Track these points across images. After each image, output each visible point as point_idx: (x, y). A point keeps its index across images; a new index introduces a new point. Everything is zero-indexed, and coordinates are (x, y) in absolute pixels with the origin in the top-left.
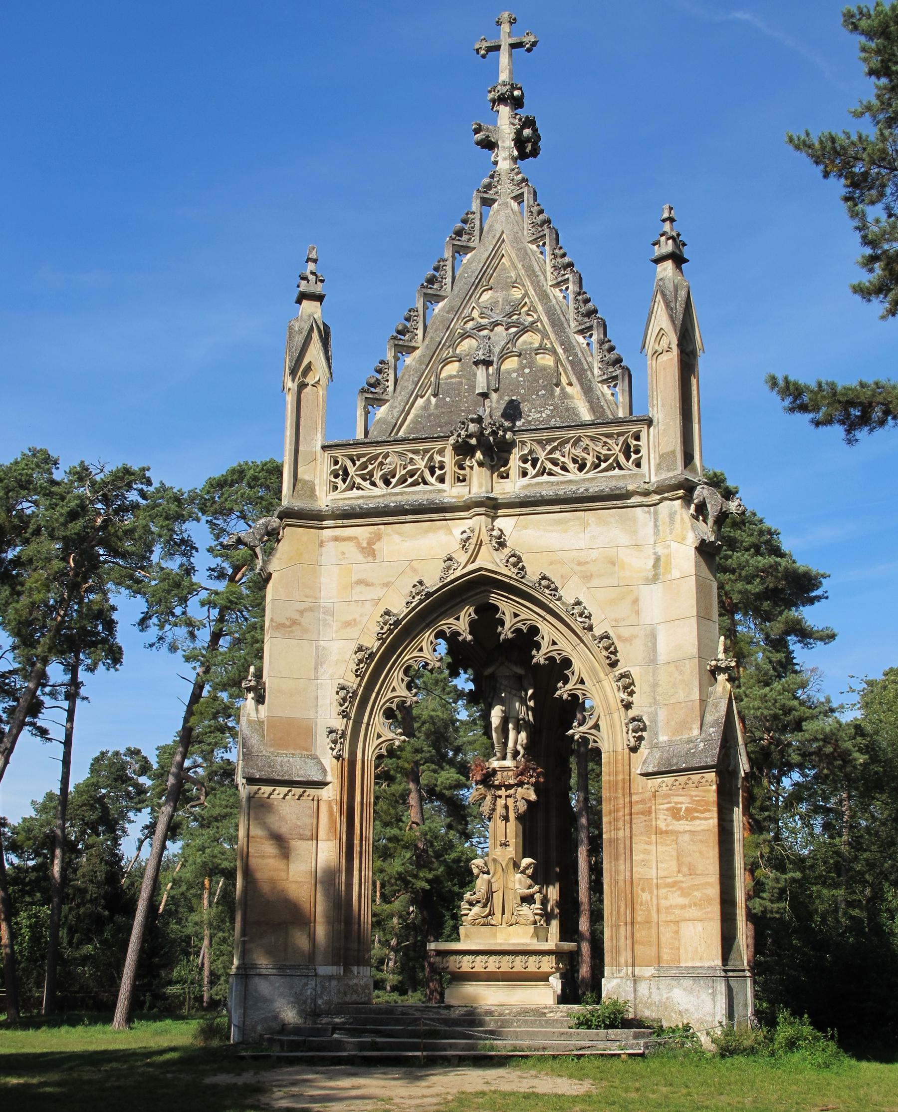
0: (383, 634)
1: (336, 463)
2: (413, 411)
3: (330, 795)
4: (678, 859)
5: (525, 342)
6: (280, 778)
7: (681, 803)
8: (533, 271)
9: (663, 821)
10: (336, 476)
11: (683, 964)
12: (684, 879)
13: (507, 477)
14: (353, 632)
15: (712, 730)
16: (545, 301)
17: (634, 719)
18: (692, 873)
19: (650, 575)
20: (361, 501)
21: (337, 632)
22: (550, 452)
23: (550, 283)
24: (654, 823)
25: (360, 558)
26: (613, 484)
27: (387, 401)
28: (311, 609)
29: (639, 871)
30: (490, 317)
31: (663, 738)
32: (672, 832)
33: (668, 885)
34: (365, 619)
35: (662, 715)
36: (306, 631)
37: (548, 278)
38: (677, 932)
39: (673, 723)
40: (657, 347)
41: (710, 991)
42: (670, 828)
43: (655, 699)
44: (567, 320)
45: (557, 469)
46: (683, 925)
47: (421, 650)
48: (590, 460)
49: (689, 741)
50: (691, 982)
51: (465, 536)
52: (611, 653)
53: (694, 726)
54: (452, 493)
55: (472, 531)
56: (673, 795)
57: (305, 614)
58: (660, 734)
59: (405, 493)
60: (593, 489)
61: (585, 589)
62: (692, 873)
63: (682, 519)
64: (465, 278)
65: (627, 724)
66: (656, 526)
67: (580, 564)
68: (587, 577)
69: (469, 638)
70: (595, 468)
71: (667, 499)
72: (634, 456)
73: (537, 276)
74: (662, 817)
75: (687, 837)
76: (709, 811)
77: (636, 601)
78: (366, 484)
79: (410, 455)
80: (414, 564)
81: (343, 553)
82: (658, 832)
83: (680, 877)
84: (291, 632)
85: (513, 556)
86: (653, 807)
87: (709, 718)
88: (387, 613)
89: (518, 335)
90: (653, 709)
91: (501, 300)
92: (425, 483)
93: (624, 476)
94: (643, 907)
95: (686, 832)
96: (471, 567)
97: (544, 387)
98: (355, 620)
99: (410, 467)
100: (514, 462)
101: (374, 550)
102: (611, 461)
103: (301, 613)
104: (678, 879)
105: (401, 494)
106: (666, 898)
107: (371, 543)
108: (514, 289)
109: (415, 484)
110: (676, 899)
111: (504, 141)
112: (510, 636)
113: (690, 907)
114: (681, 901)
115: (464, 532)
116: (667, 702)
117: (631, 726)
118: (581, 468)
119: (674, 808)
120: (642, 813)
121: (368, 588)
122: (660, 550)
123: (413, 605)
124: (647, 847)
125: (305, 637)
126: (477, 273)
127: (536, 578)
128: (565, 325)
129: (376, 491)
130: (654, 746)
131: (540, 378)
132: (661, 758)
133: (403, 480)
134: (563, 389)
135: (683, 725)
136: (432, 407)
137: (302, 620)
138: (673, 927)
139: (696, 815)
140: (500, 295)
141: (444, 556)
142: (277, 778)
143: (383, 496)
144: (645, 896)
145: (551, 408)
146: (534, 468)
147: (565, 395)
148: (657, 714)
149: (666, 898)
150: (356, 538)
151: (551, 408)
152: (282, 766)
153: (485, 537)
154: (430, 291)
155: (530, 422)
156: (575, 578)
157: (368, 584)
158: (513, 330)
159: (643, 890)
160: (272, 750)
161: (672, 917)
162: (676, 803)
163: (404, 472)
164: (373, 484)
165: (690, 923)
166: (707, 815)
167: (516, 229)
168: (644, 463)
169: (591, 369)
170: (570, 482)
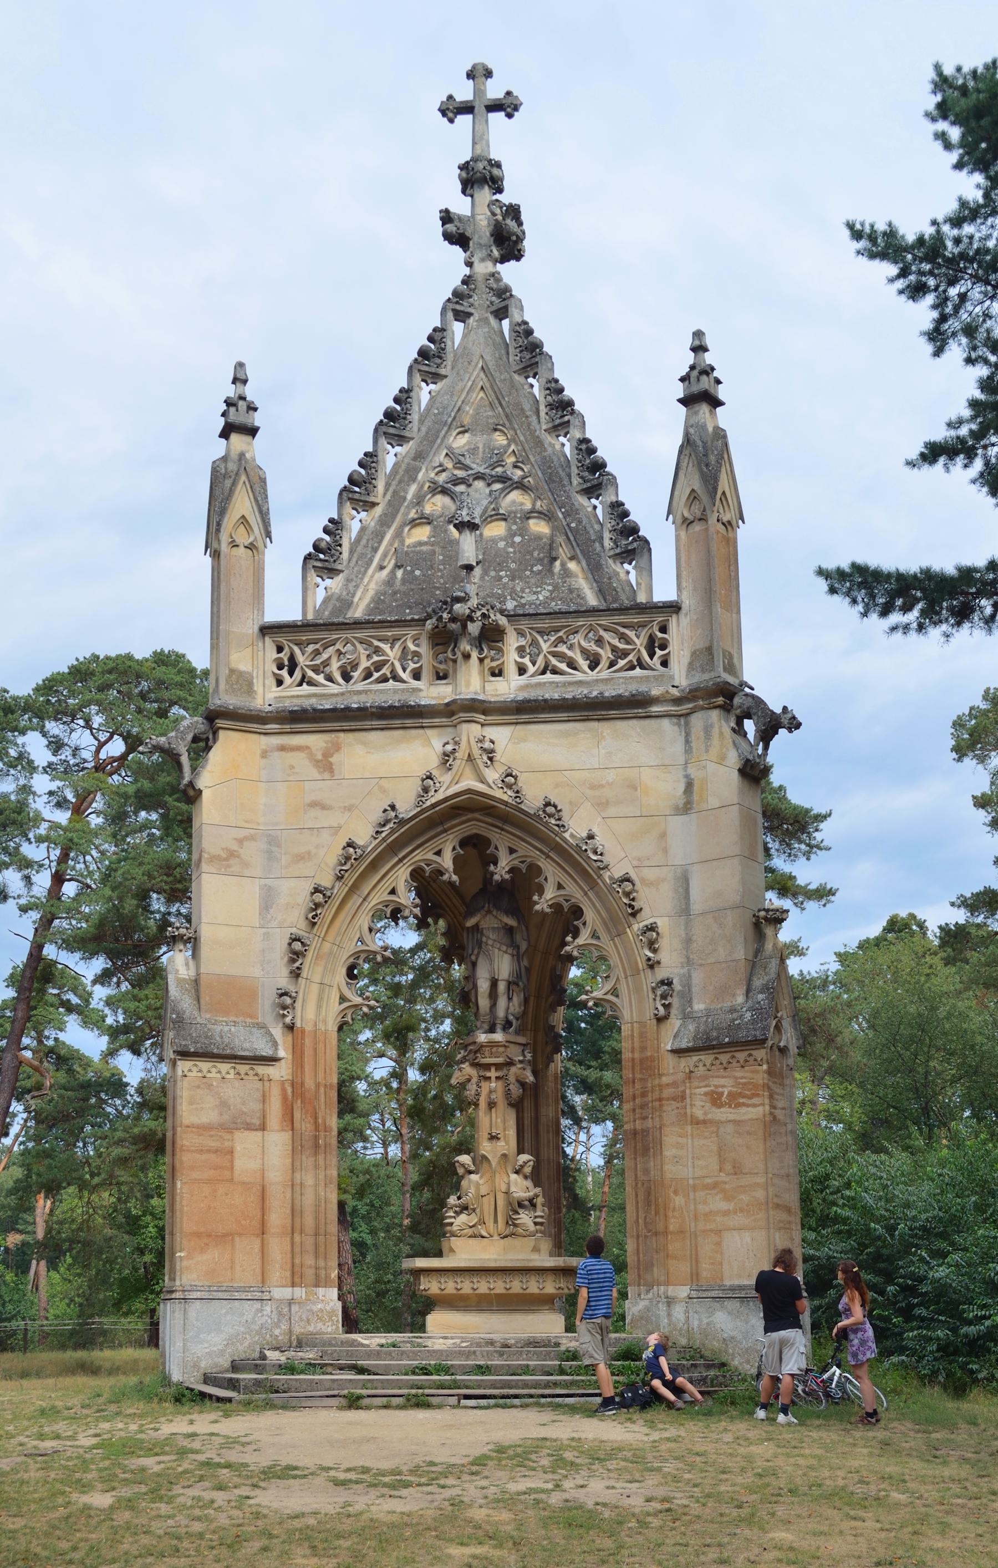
0: (346, 871)
1: (280, 649)
3: (283, 1074)
4: (720, 1156)
5: (514, 502)
7: (723, 1086)
8: (522, 409)
9: (699, 1108)
10: (280, 667)
11: (728, 1283)
12: (727, 1179)
15: (761, 997)
16: (538, 449)
17: (662, 983)
18: (737, 1170)
19: (681, 803)
20: (313, 701)
21: (286, 867)
23: (544, 427)
24: (688, 1111)
25: (315, 774)
26: (633, 688)
27: (342, 571)
28: (252, 838)
29: (671, 1170)
30: (466, 468)
33: (707, 1187)
35: (697, 978)
36: (246, 865)
37: (543, 420)
38: (719, 1244)
39: (711, 988)
42: (710, 1116)
43: (688, 958)
44: (569, 476)
45: (563, 666)
48: (606, 655)
49: (732, 1010)
50: (738, 1304)
51: (449, 748)
53: (738, 992)
55: (457, 743)
56: (713, 1077)
57: (245, 843)
58: (695, 1001)
59: (370, 691)
60: (609, 692)
61: (600, 819)
62: (737, 1170)
63: (721, 733)
64: (435, 414)
65: (654, 989)
66: (687, 742)
67: (593, 787)
68: (601, 805)
70: (609, 668)
71: (703, 708)
72: (659, 653)
73: (527, 417)
74: (698, 1103)
75: (730, 1128)
76: (758, 1095)
77: (663, 835)
78: (320, 678)
79: (376, 643)
80: (382, 782)
81: (292, 767)
82: (696, 1122)
83: (723, 1177)
84: (229, 866)
85: (510, 775)
86: (688, 1091)
87: (758, 983)
88: (350, 844)
90: (685, 970)
91: (481, 446)
92: (396, 678)
93: (647, 677)
95: (730, 1121)
97: (540, 561)
98: (309, 853)
99: (376, 658)
100: (511, 658)
101: (331, 764)
102: (630, 657)
103: (241, 841)
104: (720, 1179)
105: (366, 692)
106: (705, 1203)
107: (327, 754)
108: (498, 433)
109: (384, 680)
110: (717, 1204)
113: (735, 1213)
114: (724, 1206)
116: (703, 962)
117: (659, 992)
118: (594, 663)
119: (713, 1092)
120: (674, 1099)
121: (325, 812)
122: (692, 771)
123: (383, 835)
124: (680, 1140)
125: (246, 873)
126: (449, 409)
127: (540, 803)
128: (566, 482)
129: (333, 689)
130: (686, 1017)
131: (534, 550)
132: (697, 1032)
133: (368, 675)
134: (563, 565)
136: (398, 582)
139: (741, 1100)
140: (480, 440)
141: (422, 773)
142: (215, 1051)
143: (342, 694)
144: (678, 1201)
145: (550, 588)
146: (534, 664)
147: (566, 573)
148: (690, 976)
149: (705, 1203)
150: (308, 748)
151: (550, 588)
152: (222, 1037)
154: (392, 431)
155: (523, 605)
156: (588, 805)
157: (324, 807)
158: (497, 486)
159: (676, 1193)
160: (208, 1016)
161: (713, 1226)
162: (716, 1086)
163: (368, 664)
164: (330, 679)
165: (735, 1233)
166: (756, 1101)
168: (673, 662)
170: (580, 683)
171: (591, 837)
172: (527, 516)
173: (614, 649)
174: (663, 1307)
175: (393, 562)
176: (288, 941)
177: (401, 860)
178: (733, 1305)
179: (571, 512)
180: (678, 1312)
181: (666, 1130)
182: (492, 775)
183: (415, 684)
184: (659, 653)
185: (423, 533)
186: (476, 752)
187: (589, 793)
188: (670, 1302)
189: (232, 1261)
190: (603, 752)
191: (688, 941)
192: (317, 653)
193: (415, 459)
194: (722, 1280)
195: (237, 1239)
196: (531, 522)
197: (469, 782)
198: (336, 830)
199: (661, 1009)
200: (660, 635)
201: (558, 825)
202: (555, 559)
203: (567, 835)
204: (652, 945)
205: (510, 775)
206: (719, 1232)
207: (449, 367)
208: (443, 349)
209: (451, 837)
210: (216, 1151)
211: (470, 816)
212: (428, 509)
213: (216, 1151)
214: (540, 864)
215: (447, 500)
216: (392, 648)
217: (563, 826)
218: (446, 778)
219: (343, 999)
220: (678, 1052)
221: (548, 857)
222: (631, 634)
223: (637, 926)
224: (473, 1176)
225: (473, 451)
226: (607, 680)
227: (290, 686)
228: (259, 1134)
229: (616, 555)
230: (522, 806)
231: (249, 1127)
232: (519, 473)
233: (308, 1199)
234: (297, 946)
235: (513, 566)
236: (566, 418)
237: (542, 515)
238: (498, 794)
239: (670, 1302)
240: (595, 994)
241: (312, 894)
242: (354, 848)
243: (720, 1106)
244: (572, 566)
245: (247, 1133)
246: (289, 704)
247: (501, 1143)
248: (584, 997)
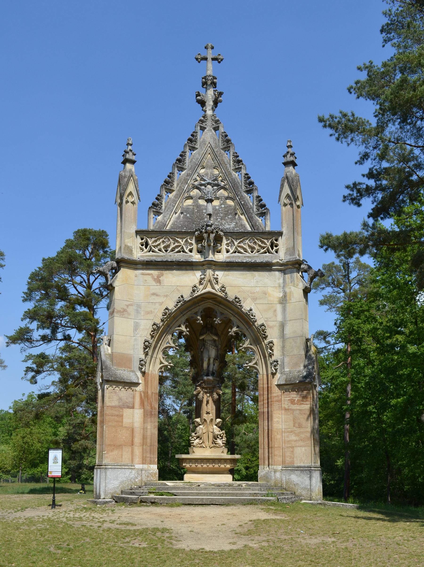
1: (142, 239)
2: (172, 219)
5: (221, 193)
6: (120, 380)
10: (142, 245)
11: (296, 465)
13: (220, 252)
14: (151, 317)
17: (275, 361)
22: (239, 243)
23: (232, 168)
24: (283, 405)
25: (154, 283)
27: (162, 213)
30: (205, 180)
31: (287, 370)
32: (290, 409)
34: (156, 311)
35: (286, 360)
38: (293, 452)
39: (291, 364)
41: (308, 476)
42: (290, 408)
45: (242, 251)
46: (295, 448)
54: (197, 257)
58: (285, 368)
61: (254, 304)
62: (300, 426)
68: (254, 299)
72: (275, 248)
73: (226, 164)
75: (298, 412)
77: (275, 311)
80: (178, 287)
81: (146, 281)
82: (286, 409)
85: (223, 287)
86: (283, 399)
88: (167, 309)
89: (219, 190)
90: (282, 357)
92: (184, 251)
94: (277, 441)
96: (204, 291)
98: (151, 311)
100: (224, 246)
101: (160, 280)
102: (265, 249)
103: (128, 306)
106: (288, 437)
107: (159, 277)
109: (179, 252)
111: (209, 102)
120: (277, 401)
123: (178, 306)
125: (129, 317)
127: (234, 298)
129: (161, 254)
134: (239, 216)
135: (297, 364)
137: (128, 309)
138: (291, 449)
140: (209, 171)
141: (192, 285)
144: (279, 437)
147: (240, 219)
148: (284, 360)
149: (288, 437)
150: (152, 274)
151: (235, 223)
154: (179, 166)
156: (249, 299)
157: (157, 295)
158: (215, 188)
160: (115, 367)
162: (293, 397)
164: (160, 250)
165: (299, 448)
169: (253, 209)
171: (251, 310)
172: (227, 198)
173: (260, 246)
174: (273, 473)
175: (180, 211)
176: (144, 342)
177: (183, 315)
178: (299, 472)
179: (242, 198)
180: (278, 475)
181: (274, 412)
182: (217, 287)
184: (275, 248)
185: (189, 202)
186: (212, 279)
187: (250, 295)
188: (275, 471)
189: (122, 455)
190: (255, 281)
191: (283, 347)
192: (156, 241)
193: (187, 176)
194: (293, 464)
195: (124, 447)
196: (227, 201)
197: (209, 289)
198: (161, 304)
199: (274, 370)
200: (275, 242)
202: (236, 214)
203: (243, 309)
204: (271, 349)
205: (223, 287)
206: (293, 447)
207: (198, 146)
208: (197, 139)
210: (117, 416)
211: (208, 301)
212: (192, 194)
213: (117, 416)
215: (198, 191)
216: (182, 241)
217: (242, 306)
218: (201, 287)
219: (161, 363)
220: (279, 386)
221: (234, 316)
222: (266, 241)
223: (266, 342)
224: (200, 426)
225: (207, 174)
226: (257, 256)
227: (146, 252)
228: (132, 410)
229: (258, 214)
230: (228, 298)
231: (128, 407)
232: (223, 183)
233: (149, 433)
234: (147, 343)
235: (221, 215)
236: (240, 166)
237: (231, 198)
238: (219, 294)
239: (275, 471)
240: (250, 364)
241: (153, 326)
242: (168, 310)
243: (294, 404)
244: (243, 217)
245: (128, 409)
246: (146, 259)
247: (211, 415)
248: (246, 365)
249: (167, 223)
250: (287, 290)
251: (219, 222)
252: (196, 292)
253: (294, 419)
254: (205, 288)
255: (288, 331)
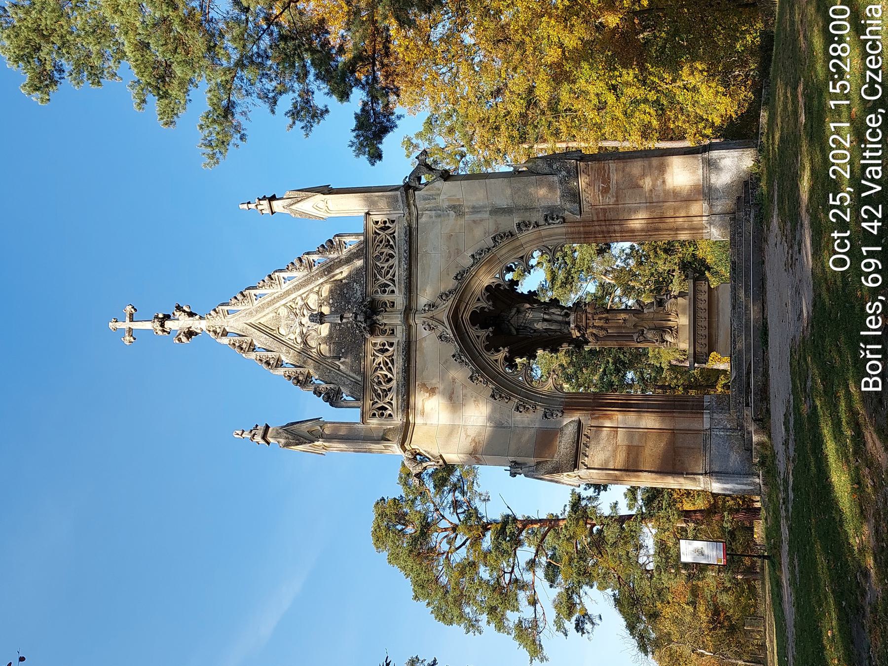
1: (374, 415)
10: (382, 414)
13: (393, 303)
17: (546, 220)
23: (279, 289)
24: (611, 206)
32: (617, 193)
37: (276, 291)
40: (324, 210)
47: (496, 361)
48: (387, 251)
51: (427, 327)
52: (504, 235)
54: (400, 335)
55: (424, 322)
65: (549, 224)
68: (458, 252)
69: (491, 329)
71: (414, 201)
76: (604, 167)
86: (601, 207)
96: (446, 323)
100: (386, 297)
109: (392, 361)
112: (490, 303)
115: (425, 328)
117: (551, 221)
118: (392, 256)
123: (467, 361)
127: (456, 282)
140: (284, 322)
145: (355, 284)
151: (355, 284)
153: (430, 314)
163: (384, 369)
166: (606, 168)
167: (243, 314)
183: (395, 344)
190: (433, 252)
201: (467, 273)
209: (470, 330)
214: (485, 285)
238: (450, 302)
249: (354, 380)
250: (445, 205)
251: (352, 307)
252: (448, 336)
253: (631, 188)
254: (443, 323)
255: (503, 203)
